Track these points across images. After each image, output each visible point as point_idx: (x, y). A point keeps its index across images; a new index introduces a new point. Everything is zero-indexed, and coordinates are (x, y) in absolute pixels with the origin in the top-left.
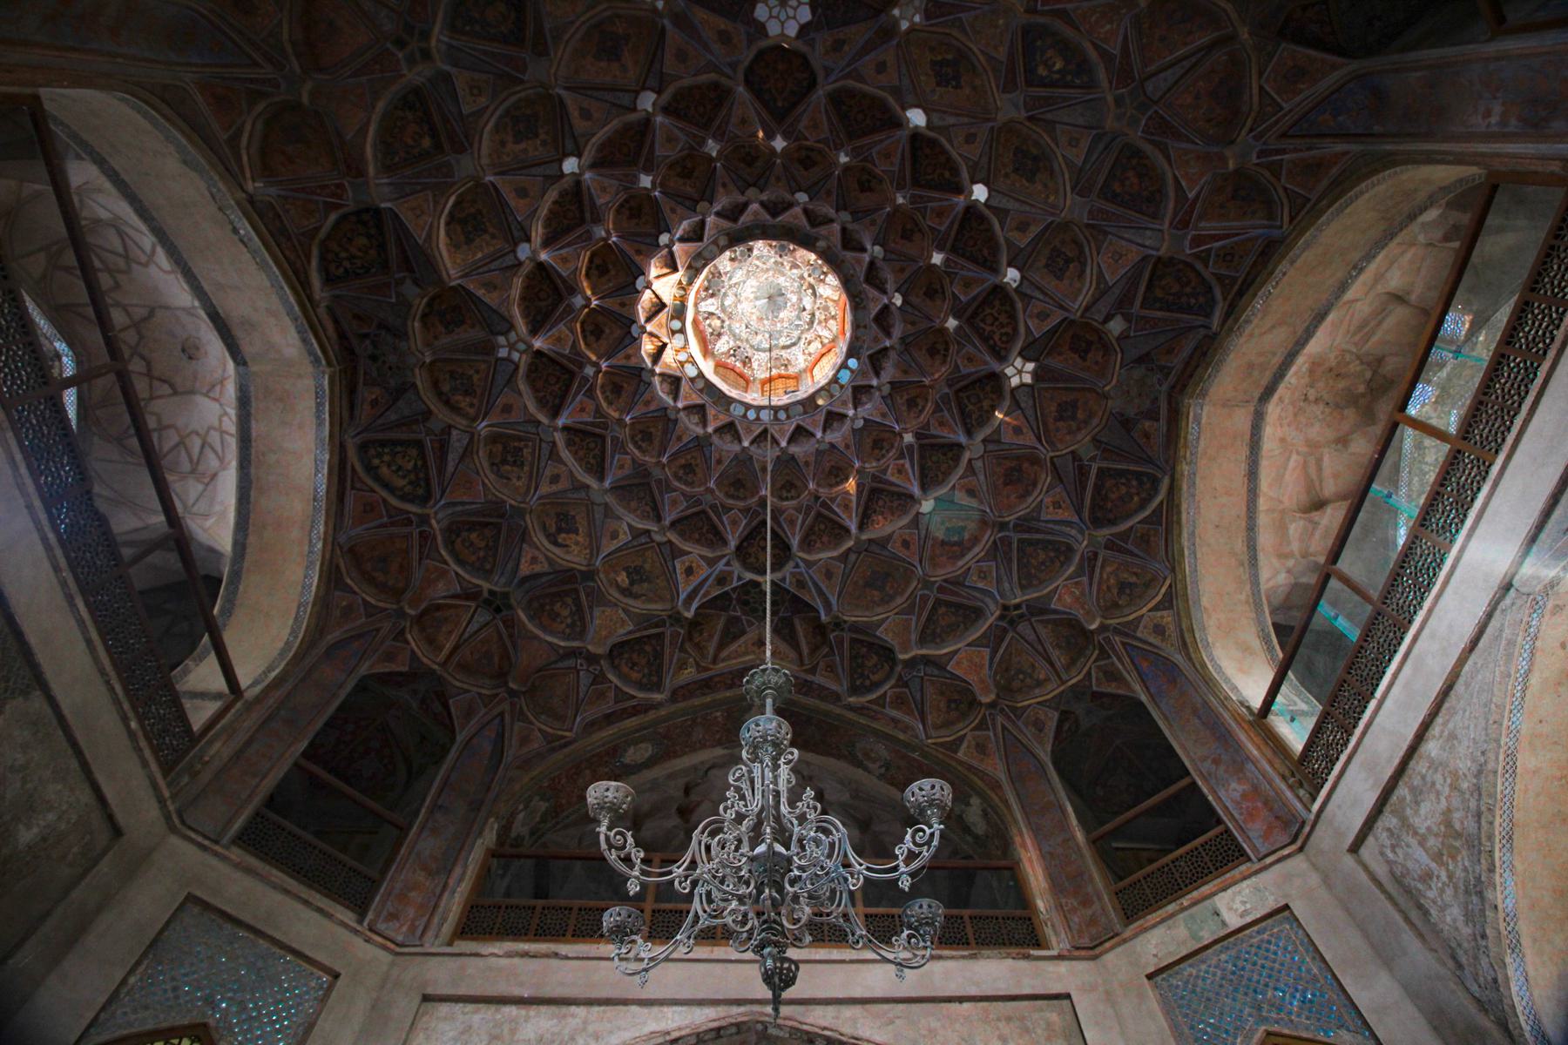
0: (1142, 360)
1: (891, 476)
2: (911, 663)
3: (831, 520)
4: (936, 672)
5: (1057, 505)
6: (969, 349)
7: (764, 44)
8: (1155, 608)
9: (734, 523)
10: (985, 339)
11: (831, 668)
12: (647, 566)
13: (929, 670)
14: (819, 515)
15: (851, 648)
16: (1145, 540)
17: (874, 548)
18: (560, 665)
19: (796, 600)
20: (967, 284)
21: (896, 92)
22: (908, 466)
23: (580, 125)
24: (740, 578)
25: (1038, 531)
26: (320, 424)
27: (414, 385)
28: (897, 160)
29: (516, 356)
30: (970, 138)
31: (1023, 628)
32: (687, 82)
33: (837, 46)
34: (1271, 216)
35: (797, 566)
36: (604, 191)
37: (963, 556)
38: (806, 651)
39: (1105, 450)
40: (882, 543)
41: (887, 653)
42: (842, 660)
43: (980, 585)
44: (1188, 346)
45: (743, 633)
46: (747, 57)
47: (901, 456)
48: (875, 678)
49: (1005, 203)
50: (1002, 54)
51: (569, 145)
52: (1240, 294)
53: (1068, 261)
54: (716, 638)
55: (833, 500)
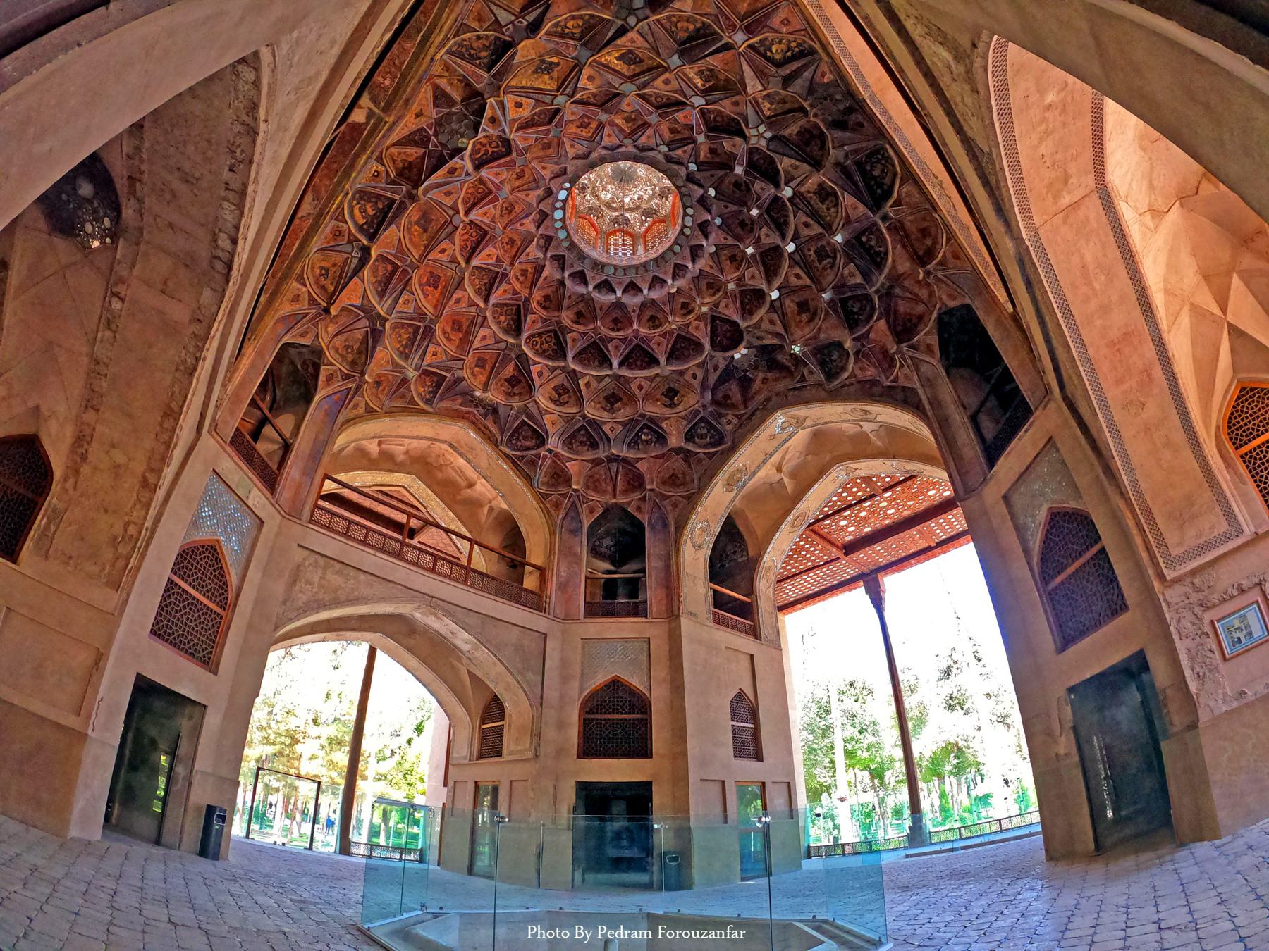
0: (495, 411)
1: (490, 250)
2: (366, 251)
3: (482, 199)
4: (353, 266)
5: (435, 354)
6: (540, 325)
7: (744, 344)
8: (367, 403)
9: (526, 139)
10: (540, 335)
11: (377, 175)
12: (547, 77)
13: (355, 261)
14: (490, 192)
15: (387, 197)
16: (403, 396)
17: (450, 228)
18: (538, 11)
19: (441, 162)
20: (574, 340)
21: (681, 373)
22: (490, 261)
23: (798, 270)
24: (484, 130)
25: (423, 339)
26: (853, 64)
27: (806, 100)
28: (654, 347)
29: (754, 132)
30: (640, 387)
31: (365, 322)
32: (762, 312)
33: (716, 368)
34: (543, 483)
35: (468, 174)
36: (769, 237)
37: (420, 285)
38: (394, 150)
39: (455, 382)
40: (450, 236)
41: (373, 229)
42: (382, 189)
43: (401, 301)
44: (494, 429)
45: (436, 105)
46: (746, 337)
47: (498, 260)
48: (356, 211)
49: (603, 384)
50: (664, 425)
51: (797, 258)
52: (514, 462)
53: (560, 395)
54: (448, 89)
55: (495, 207)
